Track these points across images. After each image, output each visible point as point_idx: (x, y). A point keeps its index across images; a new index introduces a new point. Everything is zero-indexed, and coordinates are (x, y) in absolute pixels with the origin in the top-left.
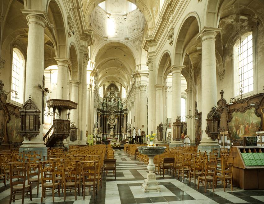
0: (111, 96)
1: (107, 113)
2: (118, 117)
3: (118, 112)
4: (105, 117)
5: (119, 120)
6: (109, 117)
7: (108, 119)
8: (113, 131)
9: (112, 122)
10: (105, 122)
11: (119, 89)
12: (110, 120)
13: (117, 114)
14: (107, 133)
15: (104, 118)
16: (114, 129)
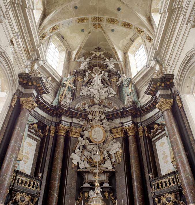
1: (75, 120)
2: (125, 133)
3: (123, 114)
5: (132, 147)
6: (82, 136)
9: (97, 158)
11: (120, 55)
12: (84, 147)
13: (118, 121)
15: (56, 137)
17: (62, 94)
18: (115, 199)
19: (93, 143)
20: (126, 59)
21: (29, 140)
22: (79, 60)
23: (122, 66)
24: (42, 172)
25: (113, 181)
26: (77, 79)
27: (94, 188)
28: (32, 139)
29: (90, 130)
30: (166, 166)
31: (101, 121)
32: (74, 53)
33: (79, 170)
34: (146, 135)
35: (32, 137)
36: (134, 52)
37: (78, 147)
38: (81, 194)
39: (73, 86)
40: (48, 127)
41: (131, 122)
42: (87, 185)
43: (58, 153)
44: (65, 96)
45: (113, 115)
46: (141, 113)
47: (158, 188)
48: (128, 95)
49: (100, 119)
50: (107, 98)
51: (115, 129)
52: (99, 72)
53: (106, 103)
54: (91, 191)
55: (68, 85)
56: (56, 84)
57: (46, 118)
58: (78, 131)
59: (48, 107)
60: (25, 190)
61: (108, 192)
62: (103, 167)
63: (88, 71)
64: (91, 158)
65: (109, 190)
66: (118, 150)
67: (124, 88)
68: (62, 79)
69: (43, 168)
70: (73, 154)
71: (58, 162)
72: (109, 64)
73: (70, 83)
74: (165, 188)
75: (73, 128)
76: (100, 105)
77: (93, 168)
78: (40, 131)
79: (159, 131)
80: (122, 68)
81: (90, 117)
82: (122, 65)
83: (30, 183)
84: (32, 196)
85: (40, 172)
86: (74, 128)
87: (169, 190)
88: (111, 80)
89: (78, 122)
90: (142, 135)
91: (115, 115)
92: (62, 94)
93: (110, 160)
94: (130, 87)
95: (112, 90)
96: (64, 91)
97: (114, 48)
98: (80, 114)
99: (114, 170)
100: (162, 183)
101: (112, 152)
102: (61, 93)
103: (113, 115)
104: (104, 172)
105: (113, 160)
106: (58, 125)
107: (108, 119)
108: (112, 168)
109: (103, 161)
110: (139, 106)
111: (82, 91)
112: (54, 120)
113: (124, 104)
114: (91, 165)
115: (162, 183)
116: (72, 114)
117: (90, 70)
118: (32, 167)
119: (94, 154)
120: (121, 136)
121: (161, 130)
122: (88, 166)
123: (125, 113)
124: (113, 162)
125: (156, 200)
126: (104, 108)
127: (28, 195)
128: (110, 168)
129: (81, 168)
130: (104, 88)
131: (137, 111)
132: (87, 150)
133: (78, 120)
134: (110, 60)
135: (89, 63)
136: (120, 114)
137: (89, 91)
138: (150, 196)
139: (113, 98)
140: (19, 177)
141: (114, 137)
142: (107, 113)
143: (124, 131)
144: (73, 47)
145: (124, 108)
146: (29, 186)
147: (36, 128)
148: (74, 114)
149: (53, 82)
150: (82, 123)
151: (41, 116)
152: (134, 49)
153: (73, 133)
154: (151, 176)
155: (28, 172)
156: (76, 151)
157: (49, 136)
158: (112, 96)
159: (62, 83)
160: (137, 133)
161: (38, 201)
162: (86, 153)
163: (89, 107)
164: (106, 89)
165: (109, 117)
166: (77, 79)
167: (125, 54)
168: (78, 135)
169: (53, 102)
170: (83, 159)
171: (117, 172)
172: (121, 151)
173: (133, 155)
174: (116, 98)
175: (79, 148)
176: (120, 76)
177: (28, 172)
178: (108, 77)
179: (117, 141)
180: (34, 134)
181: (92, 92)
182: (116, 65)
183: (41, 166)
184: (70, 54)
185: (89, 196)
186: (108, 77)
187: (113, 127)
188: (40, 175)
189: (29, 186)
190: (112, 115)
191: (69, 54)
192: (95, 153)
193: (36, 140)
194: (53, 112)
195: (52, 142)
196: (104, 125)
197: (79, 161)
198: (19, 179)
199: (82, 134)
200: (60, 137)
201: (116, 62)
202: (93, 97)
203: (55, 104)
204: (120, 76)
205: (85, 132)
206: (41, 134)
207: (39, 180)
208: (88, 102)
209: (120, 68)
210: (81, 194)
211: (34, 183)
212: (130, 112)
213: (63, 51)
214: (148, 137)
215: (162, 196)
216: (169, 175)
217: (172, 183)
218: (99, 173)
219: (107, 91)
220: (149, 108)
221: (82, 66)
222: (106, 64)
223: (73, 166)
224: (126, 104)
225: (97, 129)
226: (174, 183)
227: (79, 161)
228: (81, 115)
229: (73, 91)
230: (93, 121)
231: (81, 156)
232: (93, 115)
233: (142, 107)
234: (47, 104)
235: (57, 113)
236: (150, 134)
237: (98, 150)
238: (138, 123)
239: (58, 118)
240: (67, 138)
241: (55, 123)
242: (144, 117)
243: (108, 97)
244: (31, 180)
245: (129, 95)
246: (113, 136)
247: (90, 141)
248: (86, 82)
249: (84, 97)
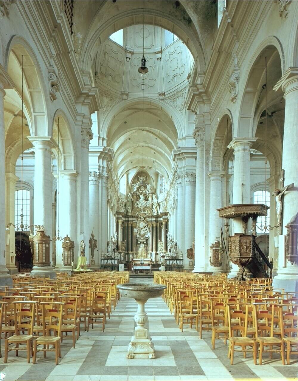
3: (152, 217)
4: (130, 225)
14: (134, 252)
15: (128, 226)
42: (139, 242)
138: (158, 246)
160: (157, 225)
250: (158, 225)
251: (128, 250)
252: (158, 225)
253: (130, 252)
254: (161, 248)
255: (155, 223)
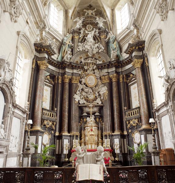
0: (87, 32)
1: (75, 71)
2: (111, 79)
3: (109, 65)
4: (67, 81)
5: (115, 89)
6: (80, 82)
7: (77, 86)
8: (96, 122)
9: (91, 97)
10: (66, 96)
11: (108, 12)
12: (82, 90)
13: (106, 70)
14: (75, 133)
15: (63, 83)
16: (100, 118)
17: (64, 51)
18: (103, 122)
19: (88, 87)
20: (113, 15)
21: (46, 87)
22: (75, 20)
23: (109, 22)
24: (56, 107)
25: (102, 112)
26: (75, 37)
27: (90, 116)
28: (48, 86)
29: (86, 78)
30: (135, 103)
31: (94, 70)
32: (71, 12)
33: (79, 105)
34: (125, 81)
35: (47, 85)
36: (120, 9)
37: (78, 90)
38: (82, 120)
39: (72, 44)
40: (57, 77)
41: (115, 72)
42: (85, 114)
43: (66, 95)
44: (67, 52)
45: (102, 66)
46: (122, 65)
47: (129, 116)
48: (113, 50)
49: (93, 69)
50: (98, 53)
51: (103, 77)
52: (92, 29)
53: (97, 57)
54: (88, 118)
55: (68, 43)
56: (59, 43)
57: (54, 71)
58: (78, 79)
59: (55, 63)
60: (49, 119)
61: (99, 118)
62: (95, 103)
63: (83, 28)
64: (87, 97)
65: (99, 117)
66: (105, 91)
67: (110, 43)
68: (63, 38)
69: (56, 104)
70: (75, 95)
71: (66, 101)
72: (99, 22)
73: (69, 42)
74: (133, 116)
75: (74, 77)
76: (93, 58)
77: (89, 103)
78: (52, 80)
79: (134, 79)
80: (110, 24)
81: (86, 67)
82: (110, 21)
83: (51, 114)
84: (53, 122)
85: (55, 107)
86: (75, 77)
87: (135, 117)
88: (101, 36)
89: (77, 72)
90: (122, 81)
91: (104, 66)
92: (64, 51)
93: (100, 98)
94: (115, 43)
95: (101, 46)
96: (66, 48)
97: (103, 7)
98: (79, 66)
99: (102, 105)
100: (131, 113)
101: (101, 93)
102: (63, 50)
103: (102, 66)
104: (96, 106)
105: (102, 98)
106: (64, 75)
107: (98, 69)
108: (101, 103)
109: (96, 99)
110: (121, 59)
111: (79, 47)
112: (60, 72)
113: (110, 58)
114: (87, 101)
115: (131, 113)
116: (72, 66)
117: (84, 28)
118: (50, 105)
119: (89, 94)
120: (107, 82)
121: (135, 78)
122: (85, 102)
123: (111, 65)
124: (102, 99)
125: (127, 122)
126: (95, 60)
127: (50, 121)
128: (100, 103)
129: (81, 103)
130: (95, 43)
131: (119, 63)
132: (84, 92)
133: (77, 70)
134: (100, 19)
135: (83, 22)
136: (107, 66)
137: (84, 47)
138: (124, 120)
139: (102, 52)
140: (44, 111)
141: (103, 82)
142: (98, 65)
143: (110, 78)
144: (69, 6)
145: (110, 62)
146: (50, 116)
147: (49, 79)
148: (74, 66)
149: (56, 42)
150: (80, 73)
151: (52, 70)
152: (120, 6)
153: (74, 80)
154: (125, 109)
155: (48, 108)
156: (77, 93)
157: (58, 83)
158: (102, 51)
159: (63, 42)
160: (118, 80)
161: (56, 124)
162: (84, 94)
163: (84, 59)
164: (97, 45)
165: (99, 68)
166: (75, 37)
167: (113, 10)
168: (77, 82)
169: (58, 57)
170: (82, 98)
171: (104, 106)
172: (107, 92)
173: (115, 95)
174: (104, 53)
175: (79, 91)
176: (108, 33)
177: (48, 108)
178: (98, 33)
179: (104, 85)
180: (48, 83)
181: (86, 48)
182: (105, 23)
183: (56, 104)
184: (67, 12)
185: (87, 121)
186: (98, 33)
187: (102, 75)
188: (56, 109)
189: (50, 116)
190: (101, 66)
191: (66, 12)
192: (90, 93)
193: (50, 86)
194: (59, 66)
195: (60, 88)
196: (96, 74)
197: (80, 99)
198: (44, 113)
199: (81, 81)
200: (65, 84)
201: (105, 21)
202: (88, 52)
203: (59, 59)
204: (107, 33)
205: (82, 79)
206: (52, 82)
207: (55, 112)
208: (84, 56)
209: (109, 25)
210: (82, 120)
211: (53, 114)
212: (114, 64)
213: (61, 10)
214: (126, 82)
215: (131, 121)
216: (136, 108)
217: (137, 113)
218: (92, 107)
219: (98, 47)
220: (127, 62)
221: (77, 25)
222: (97, 23)
223: (76, 103)
224: (111, 58)
225: (92, 77)
226: (138, 113)
227: (80, 99)
228: (79, 67)
229: (72, 48)
230: (88, 71)
231: (80, 96)
232: (87, 66)
233: (123, 61)
234: (55, 60)
235: (62, 66)
236: (128, 80)
237: (91, 91)
238: (119, 72)
239: (63, 70)
240: (70, 84)
241: (61, 73)
242: (124, 68)
243: (98, 52)
244: (51, 113)
245: (114, 49)
246: (102, 82)
247: (86, 86)
248: (81, 39)
249: (80, 52)
250: (121, 79)
251: (61, 130)
252: (121, 79)
253: (66, 133)
254: (131, 122)
255: (115, 75)
